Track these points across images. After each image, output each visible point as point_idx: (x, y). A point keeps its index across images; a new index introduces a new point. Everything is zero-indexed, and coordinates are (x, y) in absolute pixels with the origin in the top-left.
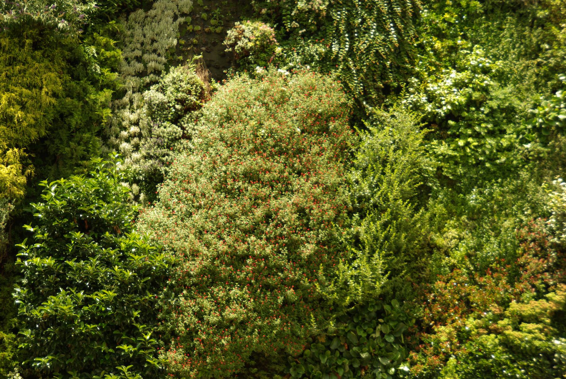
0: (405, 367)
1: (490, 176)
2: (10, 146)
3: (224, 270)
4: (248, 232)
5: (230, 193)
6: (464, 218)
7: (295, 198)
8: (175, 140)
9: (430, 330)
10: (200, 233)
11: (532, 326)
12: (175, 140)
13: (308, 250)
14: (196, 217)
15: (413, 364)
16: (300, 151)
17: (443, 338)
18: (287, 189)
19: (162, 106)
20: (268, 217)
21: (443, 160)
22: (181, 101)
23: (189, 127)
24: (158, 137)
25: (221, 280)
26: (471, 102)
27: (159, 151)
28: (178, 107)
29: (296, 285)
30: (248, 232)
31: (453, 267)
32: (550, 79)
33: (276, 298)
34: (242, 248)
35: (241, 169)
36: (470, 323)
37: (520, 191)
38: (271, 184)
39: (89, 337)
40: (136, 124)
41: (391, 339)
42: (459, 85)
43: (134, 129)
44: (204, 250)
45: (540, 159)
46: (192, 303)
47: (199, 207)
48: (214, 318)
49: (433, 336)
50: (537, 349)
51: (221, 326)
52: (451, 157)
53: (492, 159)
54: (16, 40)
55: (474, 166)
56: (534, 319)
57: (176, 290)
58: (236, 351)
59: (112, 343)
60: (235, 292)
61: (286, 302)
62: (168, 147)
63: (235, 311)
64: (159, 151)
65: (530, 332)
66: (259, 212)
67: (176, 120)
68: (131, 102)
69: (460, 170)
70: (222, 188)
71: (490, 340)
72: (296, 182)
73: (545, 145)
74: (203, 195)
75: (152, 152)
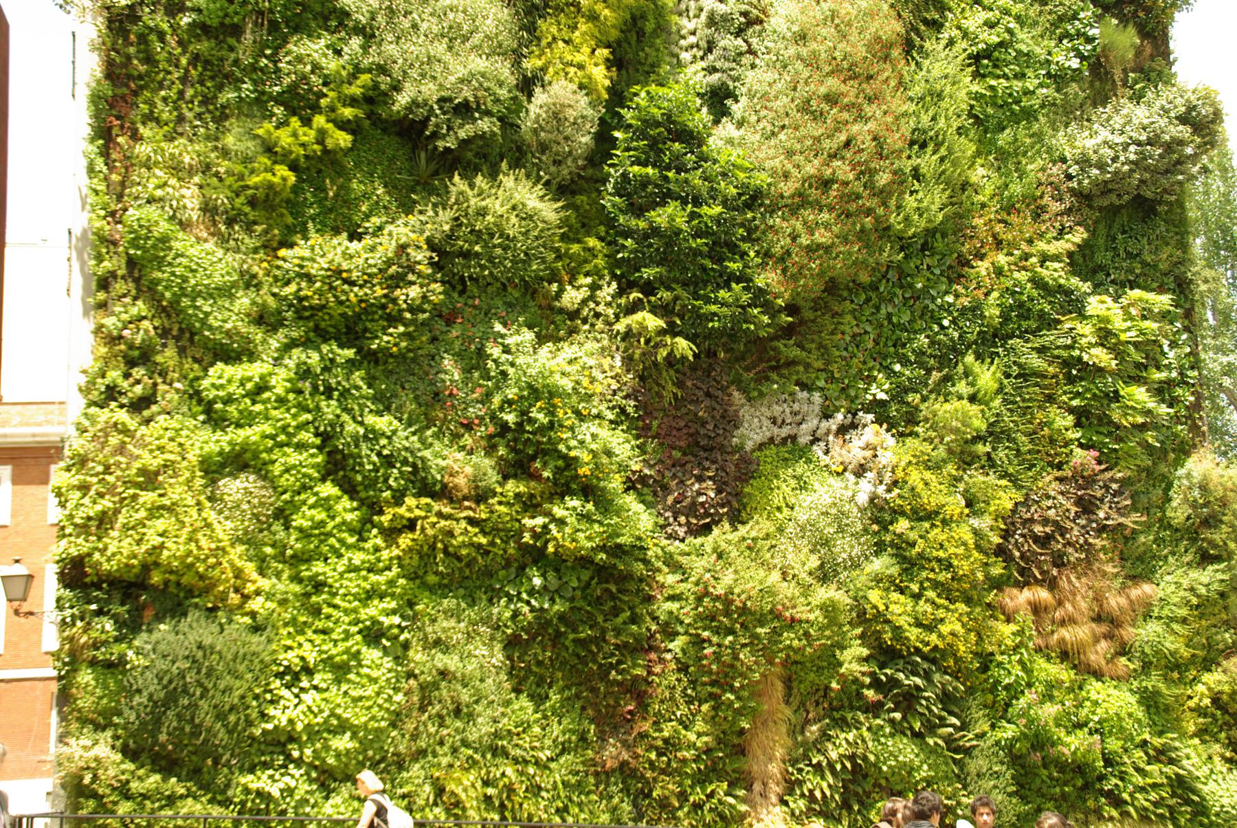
0: (950, 299)
1: (1015, 119)
2: (598, 46)
3: (814, 194)
4: (833, 156)
5: (818, 116)
6: (991, 158)
7: (871, 125)
8: (741, 54)
9: (967, 264)
10: (790, 153)
11: (1056, 265)
12: (741, 54)
13: (883, 179)
14: (782, 136)
15: (957, 296)
16: (870, 77)
17: (984, 273)
18: (861, 117)
19: (726, 18)
20: (847, 144)
21: (975, 99)
22: (745, 14)
23: (754, 41)
24: (725, 49)
25: (810, 203)
26: (1001, 44)
27: (727, 65)
28: (742, 20)
29: (869, 212)
30: (833, 156)
31: (983, 205)
32: (1057, 28)
33: (854, 224)
34: (828, 172)
35: (823, 90)
36: (1002, 259)
37: (1038, 137)
38: (847, 108)
39: (696, 252)
40: (693, 33)
41: (937, 272)
42: (991, 25)
43: (692, 40)
44: (795, 172)
45: (1054, 105)
46: (785, 225)
47: (783, 127)
48: (804, 240)
49: (972, 271)
50: (1060, 286)
51: (811, 249)
52: (983, 96)
53: (1017, 102)
55: (1002, 106)
56: (1056, 258)
57: (772, 211)
58: (821, 274)
59: (720, 260)
60: (825, 216)
61: (862, 231)
62: (734, 61)
63: (823, 236)
64: (727, 65)
65: (1055, 270)
66: (843, 137)
67: (739, 32)
68: (687, 10)
69: (990, 111)
70: (805, 108)
71: (1022, 276)
72: (869, 110)
73: (1058, 90)
74: (787, 114)
75: (718, 65)
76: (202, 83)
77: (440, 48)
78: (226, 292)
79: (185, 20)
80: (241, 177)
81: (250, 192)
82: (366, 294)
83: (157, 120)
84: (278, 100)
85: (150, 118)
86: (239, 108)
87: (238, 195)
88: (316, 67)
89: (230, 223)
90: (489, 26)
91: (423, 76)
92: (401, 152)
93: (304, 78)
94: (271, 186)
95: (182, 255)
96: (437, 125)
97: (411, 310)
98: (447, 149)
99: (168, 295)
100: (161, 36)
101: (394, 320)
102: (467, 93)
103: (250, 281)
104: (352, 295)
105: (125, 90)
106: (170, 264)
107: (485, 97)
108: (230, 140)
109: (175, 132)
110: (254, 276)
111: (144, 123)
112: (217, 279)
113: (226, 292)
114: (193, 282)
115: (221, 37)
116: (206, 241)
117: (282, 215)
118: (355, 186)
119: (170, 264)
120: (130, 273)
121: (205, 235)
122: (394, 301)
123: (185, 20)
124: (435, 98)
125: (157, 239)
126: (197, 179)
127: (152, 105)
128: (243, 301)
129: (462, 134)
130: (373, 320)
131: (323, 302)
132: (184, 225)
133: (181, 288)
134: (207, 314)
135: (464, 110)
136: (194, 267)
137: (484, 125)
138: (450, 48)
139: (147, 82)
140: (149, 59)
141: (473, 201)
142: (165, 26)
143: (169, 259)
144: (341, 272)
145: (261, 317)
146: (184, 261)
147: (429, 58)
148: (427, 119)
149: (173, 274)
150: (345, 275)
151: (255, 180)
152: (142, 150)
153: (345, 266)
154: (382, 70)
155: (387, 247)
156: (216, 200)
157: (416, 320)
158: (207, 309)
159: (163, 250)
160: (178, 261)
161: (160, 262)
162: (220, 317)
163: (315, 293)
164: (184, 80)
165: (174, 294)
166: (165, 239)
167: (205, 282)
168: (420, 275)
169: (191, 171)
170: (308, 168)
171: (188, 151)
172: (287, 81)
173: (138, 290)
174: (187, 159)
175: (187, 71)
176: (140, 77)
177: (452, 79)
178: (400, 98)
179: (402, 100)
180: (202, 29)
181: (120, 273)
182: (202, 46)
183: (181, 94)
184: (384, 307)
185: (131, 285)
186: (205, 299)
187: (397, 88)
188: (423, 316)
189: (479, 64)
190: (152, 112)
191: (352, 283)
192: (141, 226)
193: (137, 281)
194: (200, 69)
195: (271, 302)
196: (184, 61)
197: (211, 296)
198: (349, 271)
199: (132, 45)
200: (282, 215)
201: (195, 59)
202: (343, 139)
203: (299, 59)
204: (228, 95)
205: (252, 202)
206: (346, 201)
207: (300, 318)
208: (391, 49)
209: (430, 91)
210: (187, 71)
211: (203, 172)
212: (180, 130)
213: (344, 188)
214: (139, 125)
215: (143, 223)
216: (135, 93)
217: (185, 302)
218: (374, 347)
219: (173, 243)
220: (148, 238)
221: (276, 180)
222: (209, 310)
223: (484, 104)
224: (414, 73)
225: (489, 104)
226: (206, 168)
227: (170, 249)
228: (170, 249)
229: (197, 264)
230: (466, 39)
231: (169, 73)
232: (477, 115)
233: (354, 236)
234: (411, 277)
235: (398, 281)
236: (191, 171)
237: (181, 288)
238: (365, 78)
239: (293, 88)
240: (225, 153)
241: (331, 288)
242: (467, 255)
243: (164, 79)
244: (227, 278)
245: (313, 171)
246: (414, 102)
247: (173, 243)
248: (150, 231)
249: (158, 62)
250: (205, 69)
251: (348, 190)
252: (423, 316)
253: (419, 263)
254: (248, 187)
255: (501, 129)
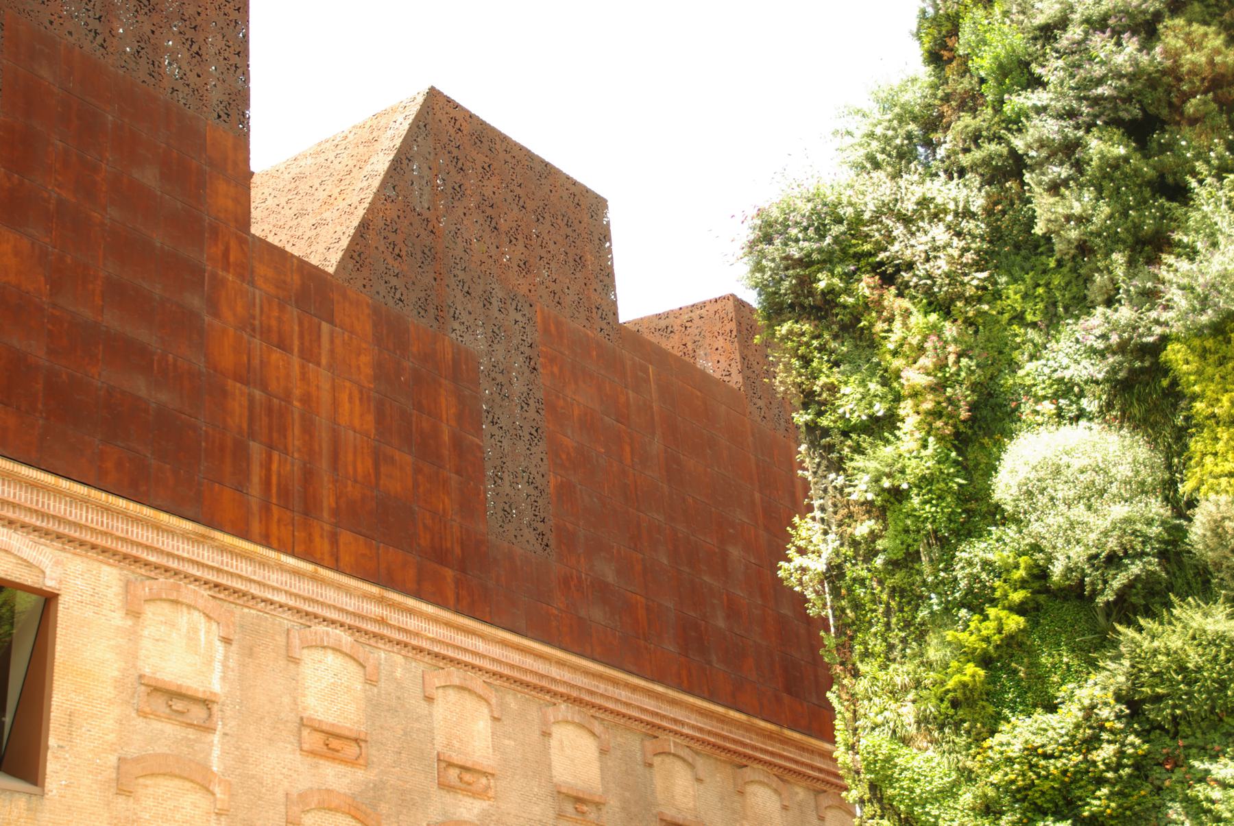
54: (1220, 338)
76: (901, 610)
77: (1079, 512)
78: (949, 792)
79: (879, 562)
80: (943, 683)
81: (950, 695)
82: (1064, 764)
83: (872, 655)
84: (962, 605)
85: (866, 655)
86: (933, 622)
87: (942, 700)
88: (986, 564)
89: (941, 728)
90: (1124, 471)
91: (1069, 542)
92: (1082, 615)
93: (976, 578)
94: (964, 685)
95: (906, 769)
96: (1092, 583)
97: (1109, 767)
98: (1108, 603)
99: (902, 807)
100: (862, 582)
101: (1100, 781)
102: (1112, 544)
103: (968, 776)
104: (1052, 768)
105: (844, 638)
106: (898, 780)
107: (1131, 541)
108: (933, 654)
109: (889, 660)
110: (971, 771)
111: (862, 661)
112: (938, 783)
113: (949, 792)
114: (918, 791)
115: (910, 565)
116: (927, 749)
117: (984, 707)
118: (1043, 660)
119: (898, 780)
120: (875, 795)
121: (925, 744)
122: (1094, 763)
123: (879, 562)
124: (1084, 557)
125: (883, 761)
126: (912, 695)
127: (865, 643)
128: (967, 797)
129: (1116, 584)
130: (1081, 787)
131: (1028, 782)
132: (906, 741)
133: (911, 799)
134: (937, 817)
135: (1113, 561)
136: (916, 777)
137: (1135, 569)
138: (1089, 508)
139: (862, 624)
140: (857, 606)
141: (1146, 644)
142: (864, 573)
143: (896, 775)
144: (1036, 749)
145: (988, 807)
146: (908, 774)
147: (1072, 524)
148: (1082, 581)
149: (902, 788)
150: (1040, 751)
151: (950, 684)
152: (862, 686)
153: (1038, 741)
154: (1036, 548)
155: (1068, 716)
156: (925, 710)
157: (1120, 777)
158: (935, 812)
159: (889, 768)
160: (903, 775)
161: (890, 780)
162: (947, 817)
163: (1018, 775)
164: (888, 612)
165: (907, 806)
166: (889, 759)
167: (928, 789)
168: (1112, 731)
169: (905, 689)
170: (1000, 657)
171: (900, 674)
172: (963, 584)
173: (882, 808)
174: (898, 681)
175: (888, 604)
176: (854, 623)
177: (1093, 536)
178: (1055, 570)
179: (1057, 570)
180: (894, 565)
181: (866, 797)
182: (898, 578)
183: (888, 624)
184: (1088, 772)
185: (877, 806)
186: (932, 804)
187: (1050, 559)
188: (1125, 772)
189: (1119, 511)
190: (867, 649)
191: (1046, 756)
192: (869, 753)
193: (880, 800)
194: (897, 599)
195: (991, 792)
196: (885, 597)
197: (936, 799)
198: (1043, 746)
199: (843, 598)
200: (984, 707)
201: (893, 591)
202: (1015, 622)
203: (970, 563)
204: (923, 614)
205: (955, 704)
206: (1039, 678)
207: (1017, 801)
208: (1036, 527)
209: (1078, 554)
210: (888, 604)
211: (916, 688)
212: (891, 657)
213: (1035, 665)
214: (859, 665)
215: (870, 749)
216: (852, 638)
217: (918, 810)
218: (1086, 814)
219: (896, 760)
220: (876, 761)
221: (966, 679)
222: (937, 813)
223: (1132, 547)
224: (1060, 542)
225: (1139, 547)
226: (918, 684)
227: (895, 766)
228: (895, 766)
229: (919, 774)
230: (1102, 493)
231: (875, 611)
232: (1126, 561)
233: (1052, 708)
234: (1105, 736)
235: (1092, 743)
236: (905, 689)
237: (911, 799)
238: (1023, 560)
239: (970, 591)
240: (929, 665)
241: (1031, 766)
242: (1158, 699)
243: (872, 618)
244: (946, 779)
245: (1005, 656)
246: (1069, 570)
247: (896, 760)
248: (877, 755)
249: (864, 605)
250: (902, 597)
251: (1037, 665)
252: (1125, 772)
253: (1107, 720)
254: (948, 691)
255: (1159, 564)
